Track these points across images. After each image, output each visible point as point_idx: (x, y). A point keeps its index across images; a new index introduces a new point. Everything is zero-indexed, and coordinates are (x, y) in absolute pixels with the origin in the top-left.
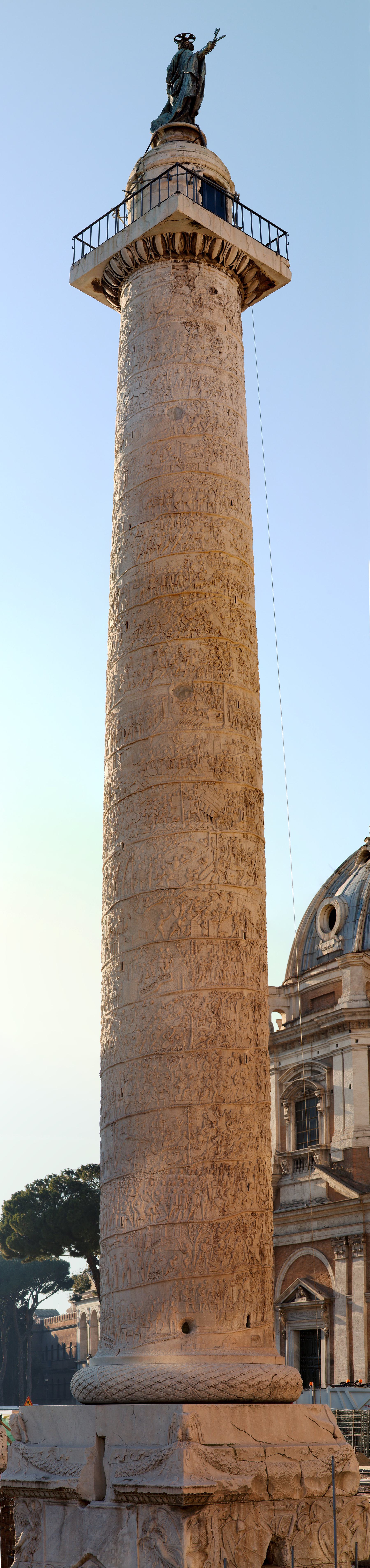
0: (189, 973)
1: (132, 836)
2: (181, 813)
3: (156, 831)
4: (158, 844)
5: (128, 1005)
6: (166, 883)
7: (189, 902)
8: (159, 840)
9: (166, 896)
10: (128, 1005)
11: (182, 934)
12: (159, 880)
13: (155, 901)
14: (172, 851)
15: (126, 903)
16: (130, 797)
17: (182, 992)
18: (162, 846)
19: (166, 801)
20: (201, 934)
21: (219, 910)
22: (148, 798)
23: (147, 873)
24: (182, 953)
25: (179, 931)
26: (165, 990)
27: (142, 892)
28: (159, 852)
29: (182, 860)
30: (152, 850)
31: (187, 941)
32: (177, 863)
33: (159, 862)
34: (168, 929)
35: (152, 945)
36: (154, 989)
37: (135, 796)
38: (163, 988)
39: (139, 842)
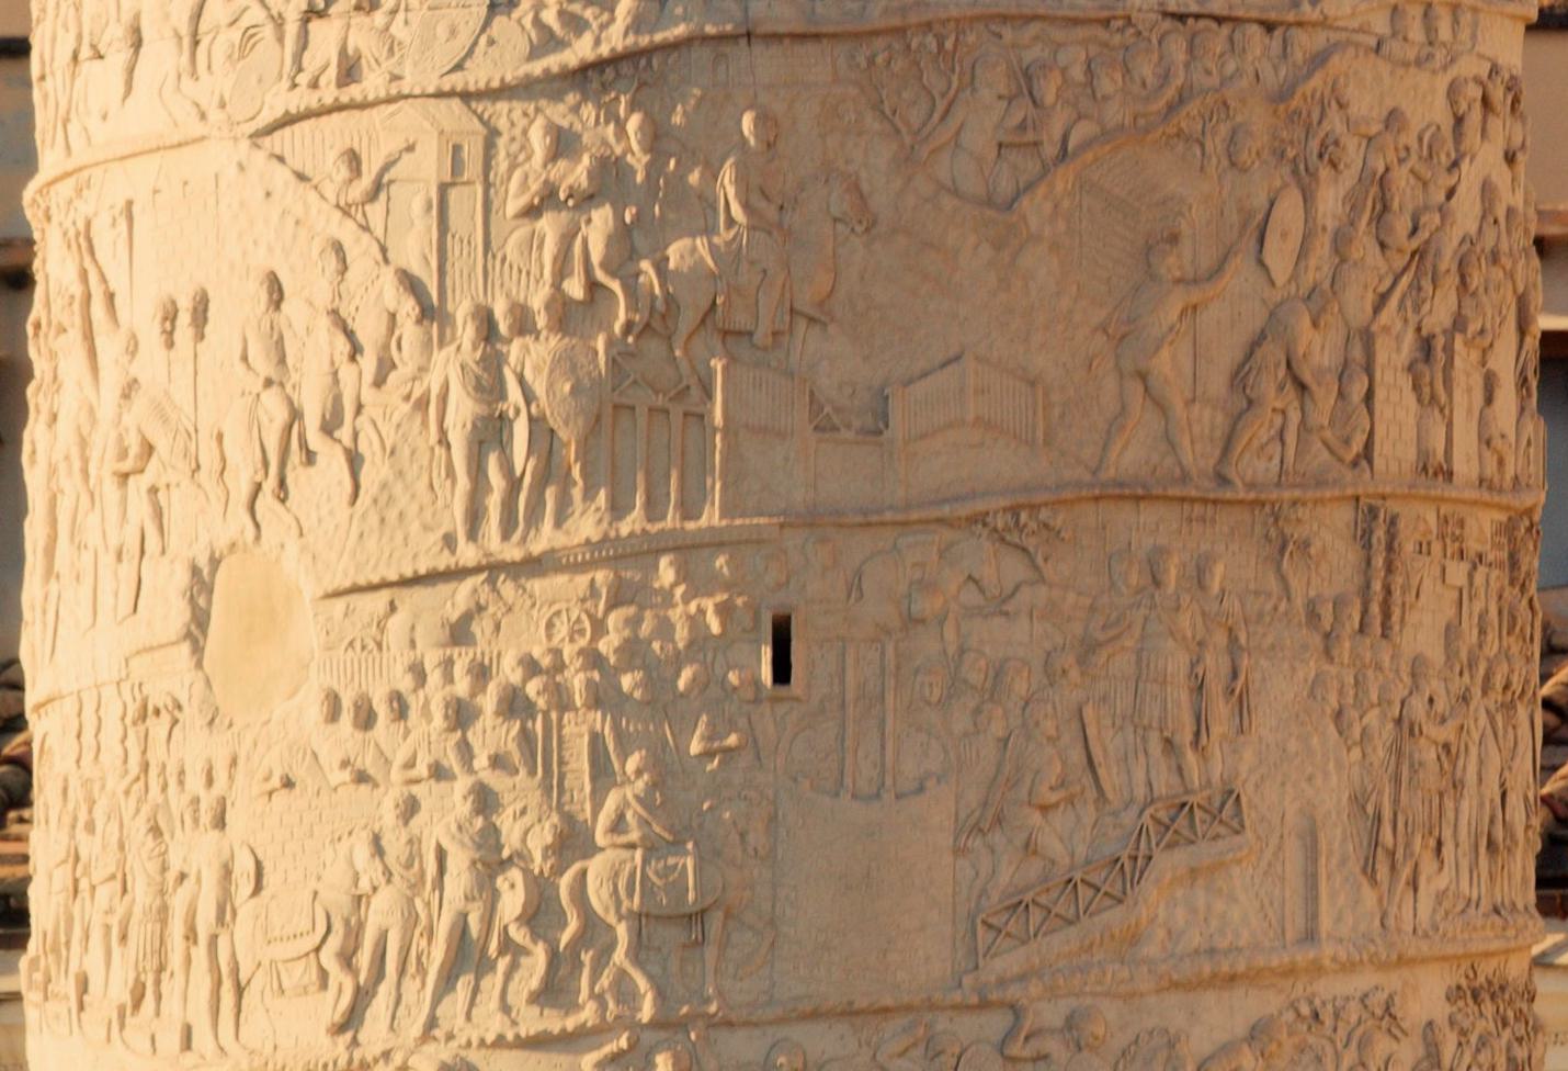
0: (1358, 801)
5: (849, 1013)
7: (1353, 151)
9: (1198, 77)
10: (849, 1013)
11: (1319, 456)
13: (1115, 113)
15: (816, 64)
17: (1317, 969)
20: (1411, 454)
21: (1489, 241)
24: (1313, 615)
25: (1294, 417)
26: (1195, 939)
31: (1343, 515)
34: (1216, 382)
35: (1090, 515)
36: (1114, 916)
38: (1180, 915)
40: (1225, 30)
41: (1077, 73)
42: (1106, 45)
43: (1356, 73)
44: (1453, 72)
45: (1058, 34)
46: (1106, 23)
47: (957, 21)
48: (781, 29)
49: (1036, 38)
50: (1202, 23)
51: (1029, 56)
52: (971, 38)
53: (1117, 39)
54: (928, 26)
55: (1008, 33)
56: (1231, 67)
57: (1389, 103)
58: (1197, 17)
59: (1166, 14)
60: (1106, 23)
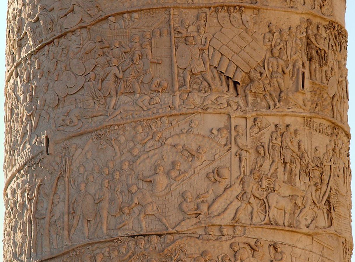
1: (67, 122)
2: (172, 73)
3: (117, 112)
4: (122, 139)
6: (139, 222)
8: (125, 130)
9: (138, 250)
12: (124, 217)
14: (151, 153)
16: (62, 40)
18: (131, 144)
19: (138, 48)
22: (101, 42)
23: (98, 202)
27: (87, 241)
28: (124, 157)
29: (173, 174)
30: (110, 152)
32: (162, 181)
33: (124, 178)
37: (74, 37)
39: (81, 135)
40: (146, 238)
41: (106, 254)
42: (114, 246)
43: (188, 243)
44: (233, 241)
45: (101, 246)
46: (112, 241)
47: (79, 247)
48: (47, 258)
49: (97, 248)
50: (139, 237)
51: (96, 252)
52: (82, 251)
53: (116, 244)
54: (73, 250)
55: (90, 247)
56: (147, 246)
57: (202, 249)
58: (138, 236)
59: (129, 236)
60: (112, 241)
